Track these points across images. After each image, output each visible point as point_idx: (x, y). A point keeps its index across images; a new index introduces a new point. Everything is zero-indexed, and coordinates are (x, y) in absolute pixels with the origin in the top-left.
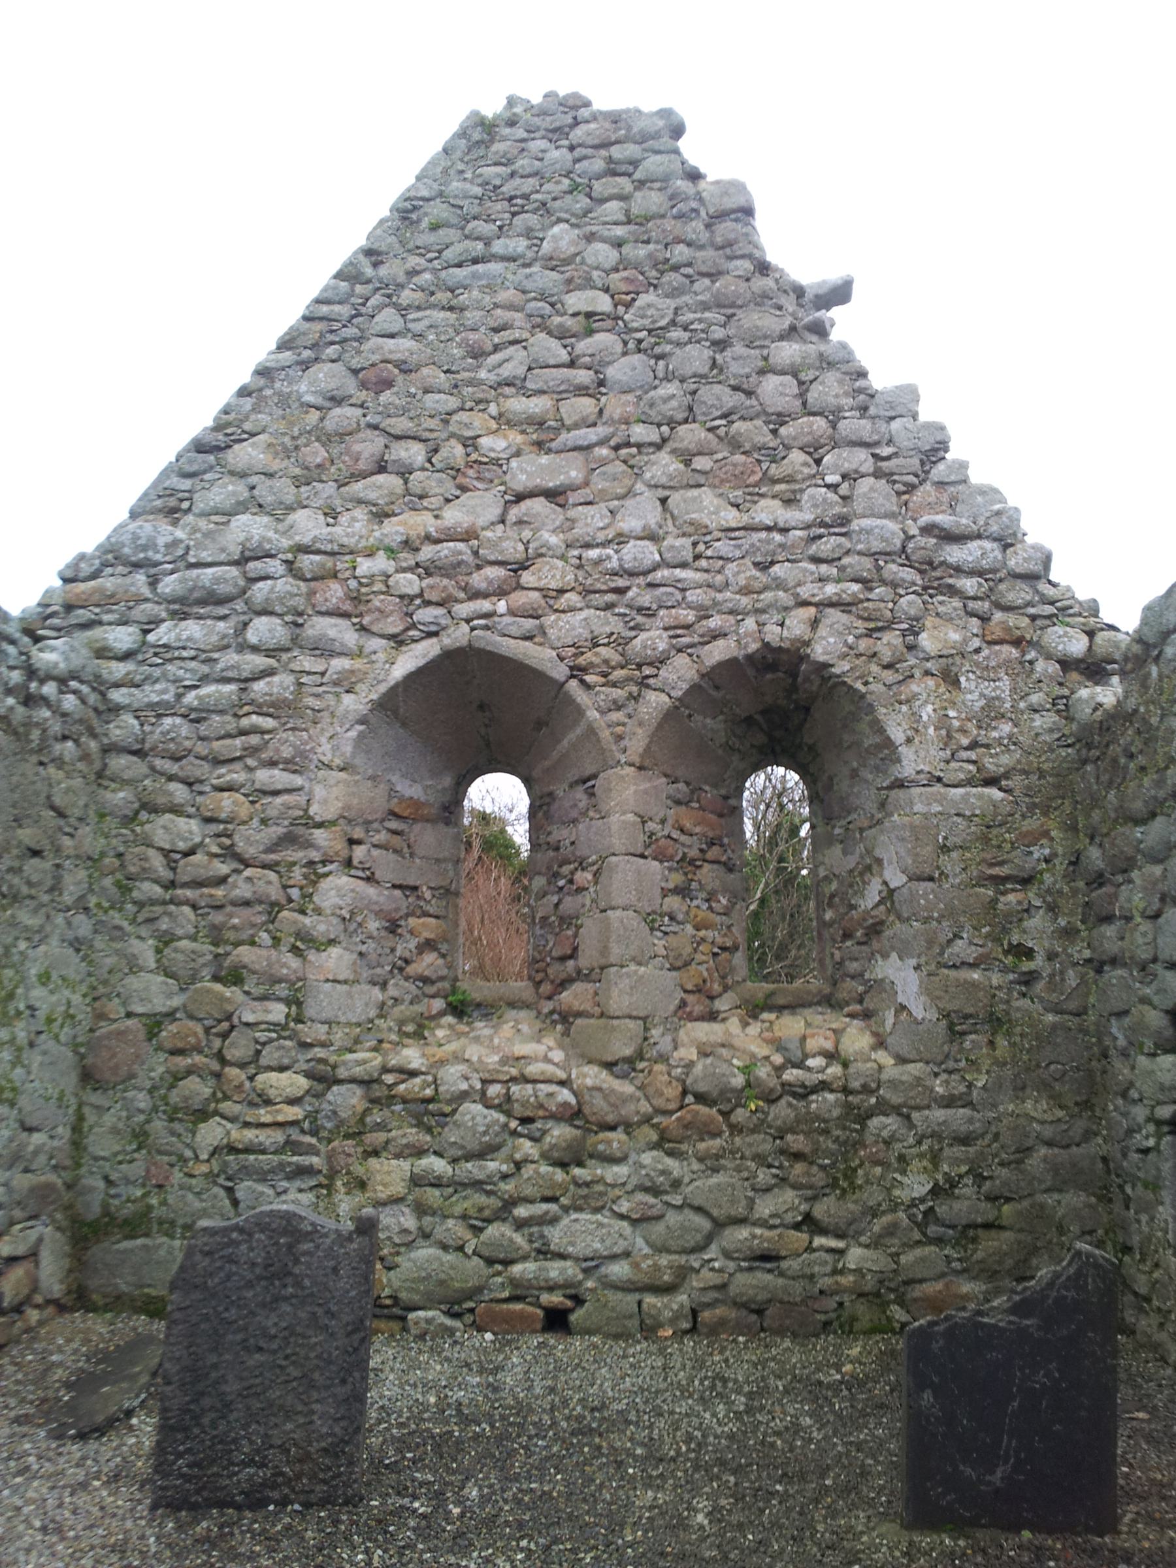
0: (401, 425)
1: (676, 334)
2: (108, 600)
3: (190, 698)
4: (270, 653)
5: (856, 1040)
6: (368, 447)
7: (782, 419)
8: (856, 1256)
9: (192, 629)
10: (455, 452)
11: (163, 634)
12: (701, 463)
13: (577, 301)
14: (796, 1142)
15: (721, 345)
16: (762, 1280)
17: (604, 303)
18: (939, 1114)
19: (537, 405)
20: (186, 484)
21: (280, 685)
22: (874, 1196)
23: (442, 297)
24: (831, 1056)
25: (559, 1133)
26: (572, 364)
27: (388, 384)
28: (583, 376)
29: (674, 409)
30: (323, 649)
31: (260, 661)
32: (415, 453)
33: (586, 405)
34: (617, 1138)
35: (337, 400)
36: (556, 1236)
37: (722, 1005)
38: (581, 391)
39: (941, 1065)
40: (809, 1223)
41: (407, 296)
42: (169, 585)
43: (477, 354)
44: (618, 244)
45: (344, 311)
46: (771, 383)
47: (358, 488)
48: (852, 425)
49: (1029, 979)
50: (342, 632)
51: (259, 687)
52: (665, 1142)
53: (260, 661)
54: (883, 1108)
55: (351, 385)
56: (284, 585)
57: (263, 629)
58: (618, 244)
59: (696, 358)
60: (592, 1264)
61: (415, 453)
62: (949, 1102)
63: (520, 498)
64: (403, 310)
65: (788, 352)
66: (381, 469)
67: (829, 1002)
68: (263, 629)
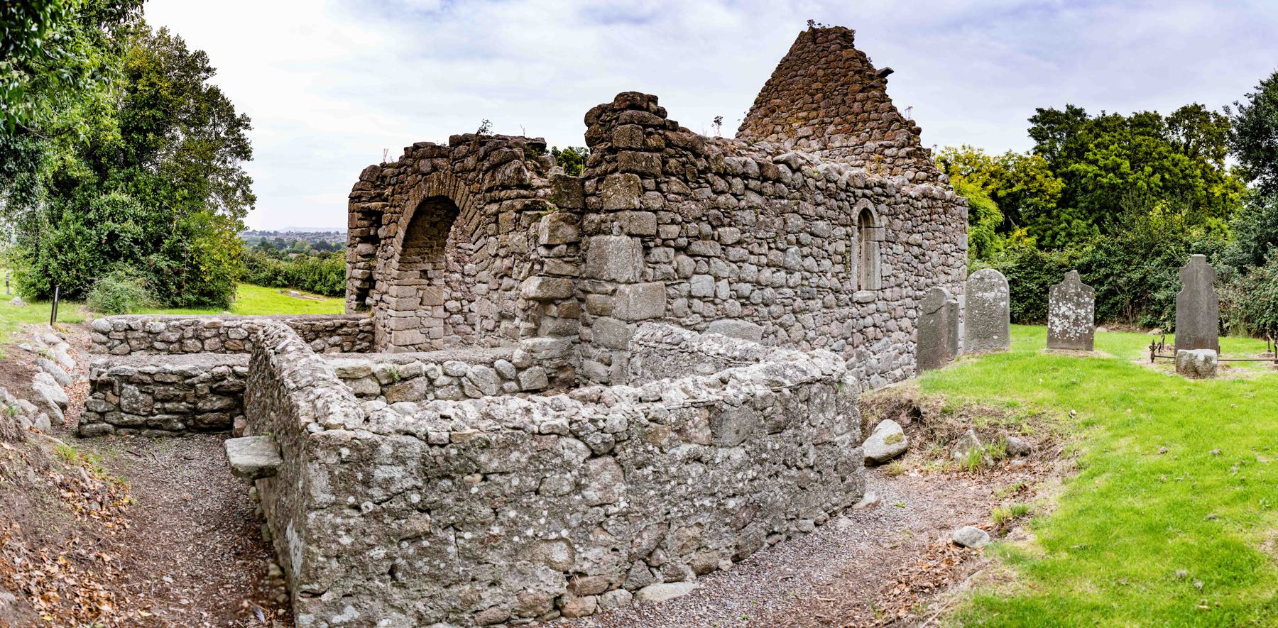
0: (778, 121)
1: (836, 93)
6: (770, 128)
7: (857, 114)
10: (787, 127)
12: (840, 127)
13: (814, 86)
15: (846, 94)
17: (820, 85)
19: (804, 114)
26: (813, 103)
27: (774, 111)
28: (815, 106)
29: (832, 114)
32: (779, 128)
33: (815, 113)
38: (815, 109)
41: (779, 88)
43: (793, 101)
44: (824, 69)
46: (856, 105)
48: (874, 115)
58: (824, 69)
59: (839, 99)
61: (779, 128)
63: (800, 138)
65: (860, 96)
66: (773, 133)
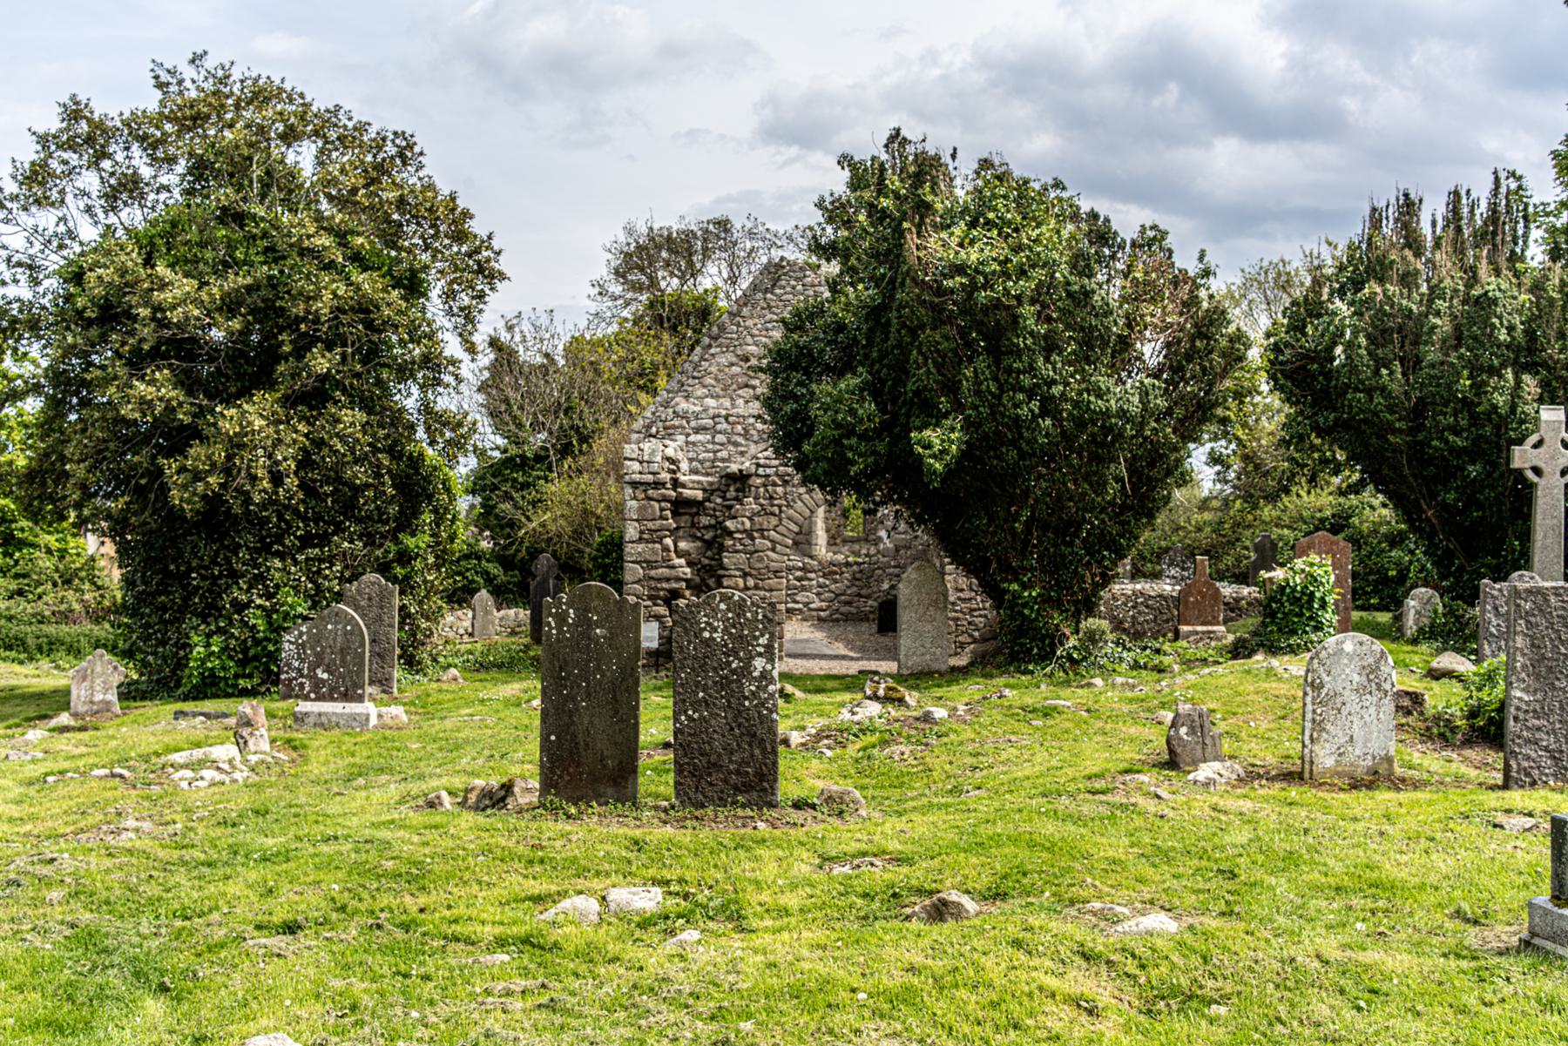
2: (674, 427)
3: (700, 457)
4: (722, 445)
5: (873, 551)
8: (870, 602)
9: (700, 437)
11: (692, 438)
14: (858, 576)
16: (844, 609)
18: (892, 570)
20: (690, 389)
21: (724, 454)
22: (875, 589)
23: (764, 333)
24: (866, 555)
25: (799, 574)
30: (736, 444)
31: (719, 447)
34: (812, 575)
35: (732, 364)
36: (798, 598)
37: (838, 541)
39: (894, 558)
40: (859, 595)
42: (693, 424)
45: (734, 336)
47: (740, 392)
49: (916, 537)
50: (740, 440)
51: (719, 454)
52: (824, 576)
53: (719, 447)
54: (879, 568)
55: (734, 360)
56: (725, 426)
57: (720, 438)
60: (806, 604)
62: (895, 567)
64: (753, 336)
67: (866, 540)
68: (720, 438)
